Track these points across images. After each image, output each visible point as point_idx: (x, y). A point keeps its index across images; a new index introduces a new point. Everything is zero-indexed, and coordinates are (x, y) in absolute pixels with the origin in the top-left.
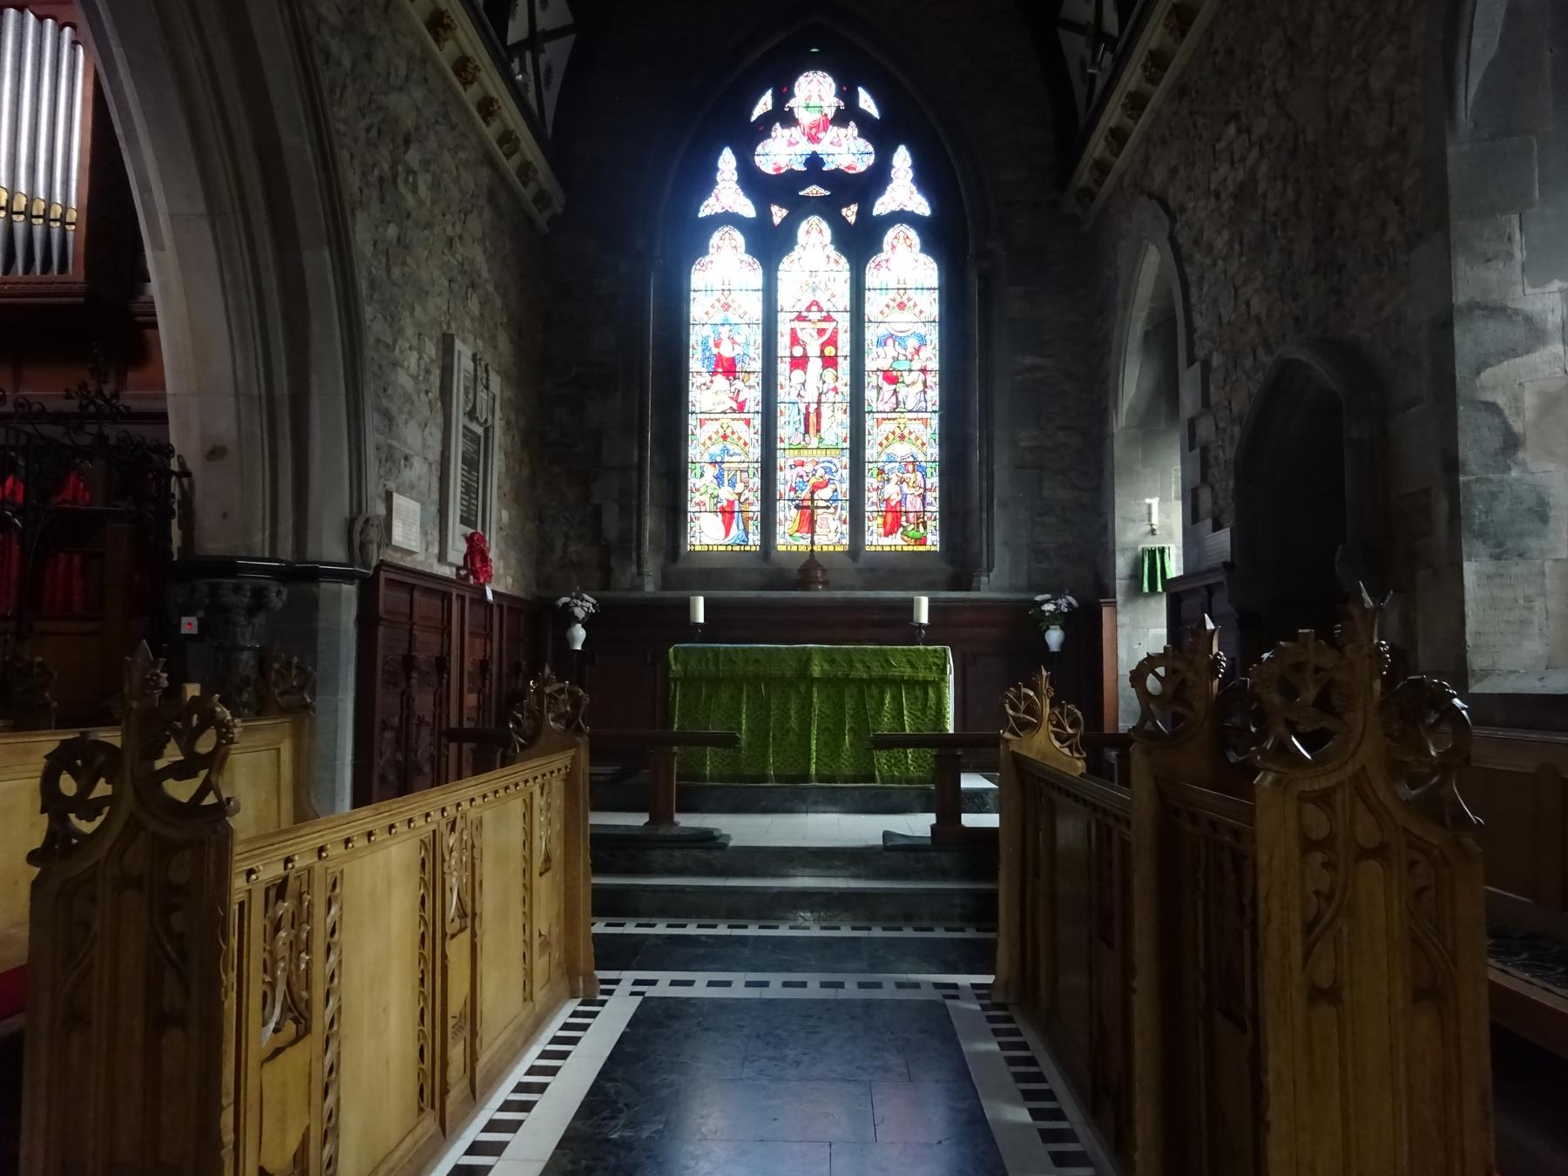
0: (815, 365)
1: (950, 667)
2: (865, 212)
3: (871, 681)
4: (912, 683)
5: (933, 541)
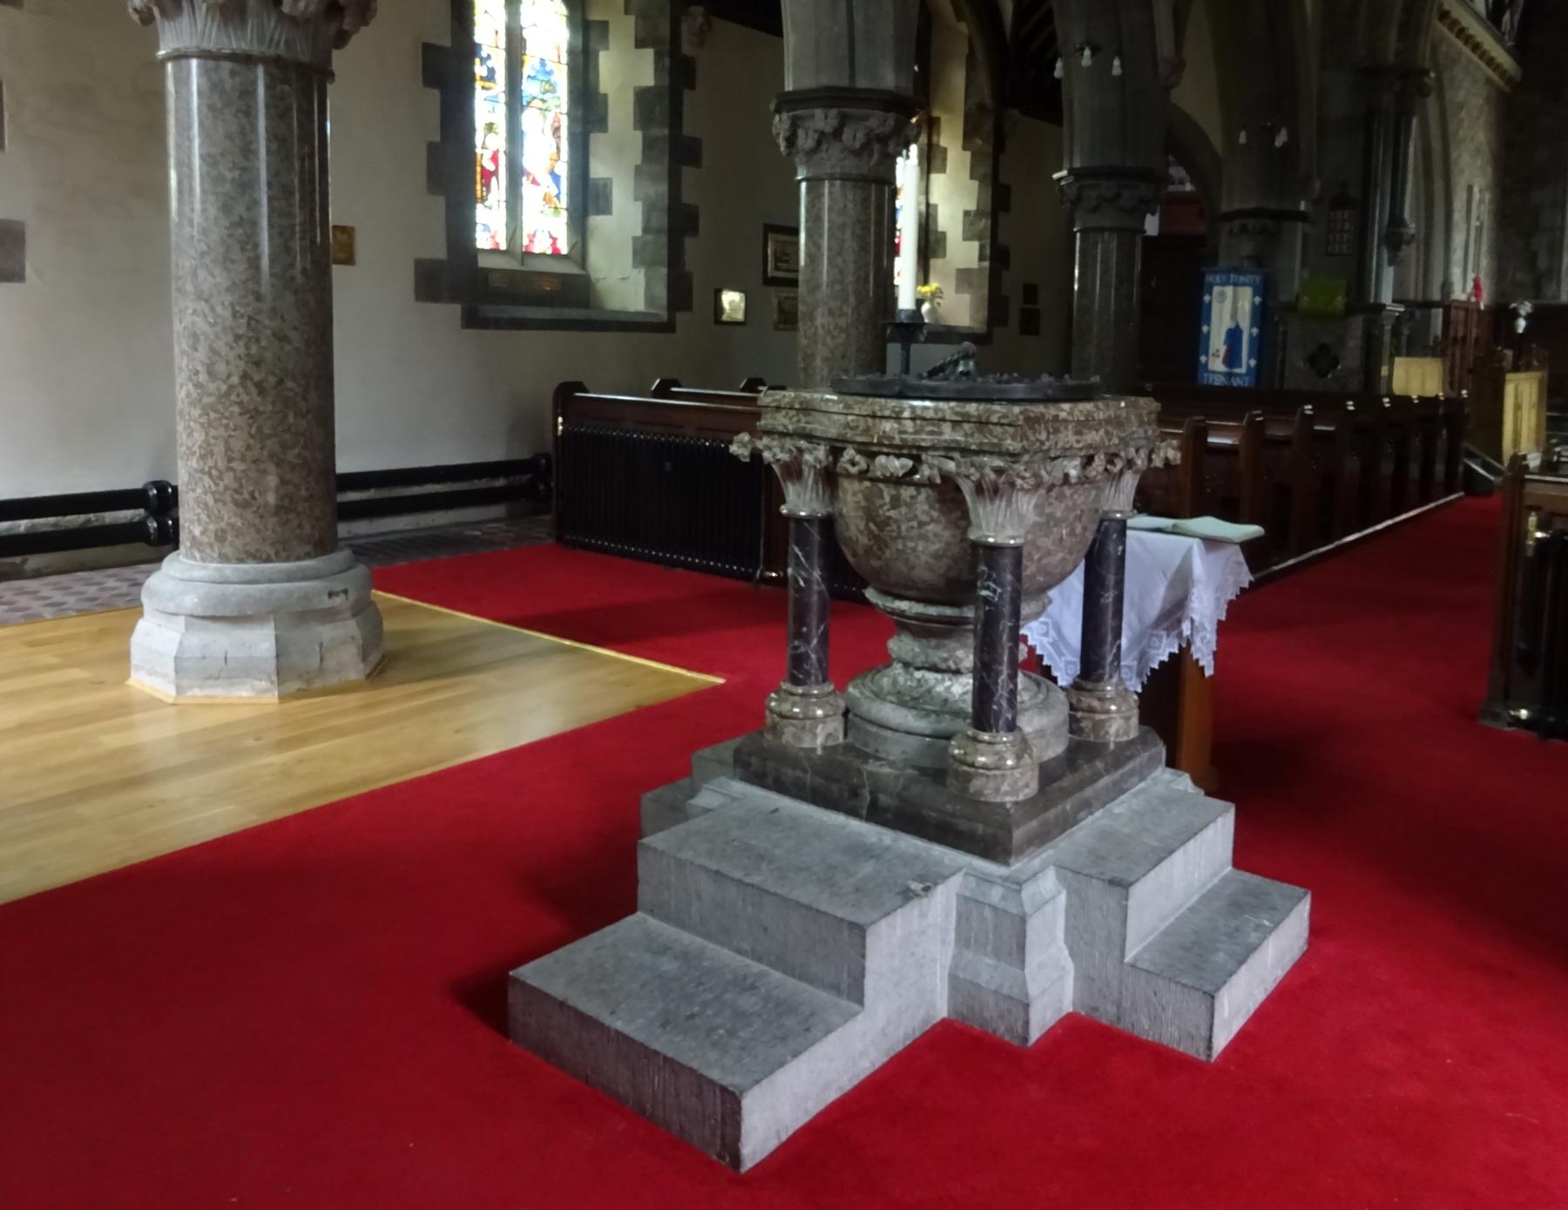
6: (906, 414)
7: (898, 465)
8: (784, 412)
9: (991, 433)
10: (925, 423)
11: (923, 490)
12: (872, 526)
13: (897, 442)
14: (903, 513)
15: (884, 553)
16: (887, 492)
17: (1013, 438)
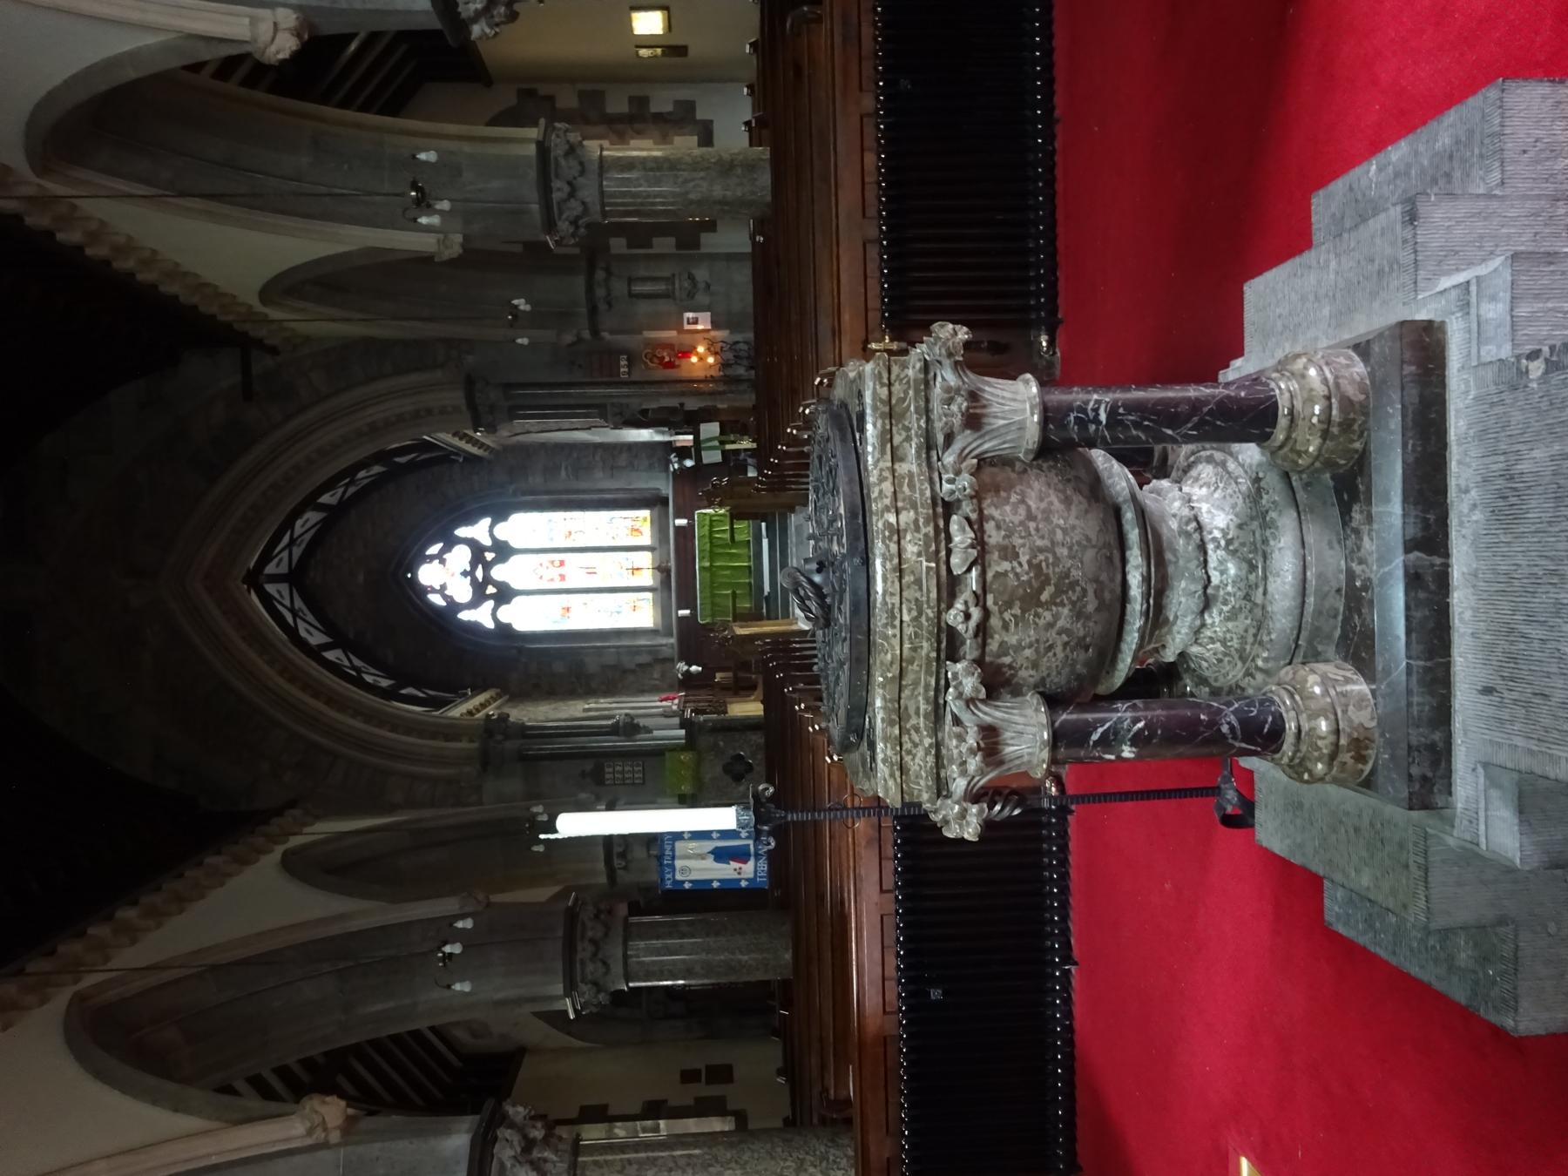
0: (562, 570)
1: (704, 511)
3: (711, 542)
4: (711, 526)
5: (646, 513)
6: (892, 518)
7: (961, 537)
8: (907, 758)
9: (904, 400)
10: (900, 496)
11: (986, 512)
12: (1045, 596)
13: (930, 529)
14: (1021, 541)
15: (1077, 583)
16: (999, 566)
17: (904, 366)
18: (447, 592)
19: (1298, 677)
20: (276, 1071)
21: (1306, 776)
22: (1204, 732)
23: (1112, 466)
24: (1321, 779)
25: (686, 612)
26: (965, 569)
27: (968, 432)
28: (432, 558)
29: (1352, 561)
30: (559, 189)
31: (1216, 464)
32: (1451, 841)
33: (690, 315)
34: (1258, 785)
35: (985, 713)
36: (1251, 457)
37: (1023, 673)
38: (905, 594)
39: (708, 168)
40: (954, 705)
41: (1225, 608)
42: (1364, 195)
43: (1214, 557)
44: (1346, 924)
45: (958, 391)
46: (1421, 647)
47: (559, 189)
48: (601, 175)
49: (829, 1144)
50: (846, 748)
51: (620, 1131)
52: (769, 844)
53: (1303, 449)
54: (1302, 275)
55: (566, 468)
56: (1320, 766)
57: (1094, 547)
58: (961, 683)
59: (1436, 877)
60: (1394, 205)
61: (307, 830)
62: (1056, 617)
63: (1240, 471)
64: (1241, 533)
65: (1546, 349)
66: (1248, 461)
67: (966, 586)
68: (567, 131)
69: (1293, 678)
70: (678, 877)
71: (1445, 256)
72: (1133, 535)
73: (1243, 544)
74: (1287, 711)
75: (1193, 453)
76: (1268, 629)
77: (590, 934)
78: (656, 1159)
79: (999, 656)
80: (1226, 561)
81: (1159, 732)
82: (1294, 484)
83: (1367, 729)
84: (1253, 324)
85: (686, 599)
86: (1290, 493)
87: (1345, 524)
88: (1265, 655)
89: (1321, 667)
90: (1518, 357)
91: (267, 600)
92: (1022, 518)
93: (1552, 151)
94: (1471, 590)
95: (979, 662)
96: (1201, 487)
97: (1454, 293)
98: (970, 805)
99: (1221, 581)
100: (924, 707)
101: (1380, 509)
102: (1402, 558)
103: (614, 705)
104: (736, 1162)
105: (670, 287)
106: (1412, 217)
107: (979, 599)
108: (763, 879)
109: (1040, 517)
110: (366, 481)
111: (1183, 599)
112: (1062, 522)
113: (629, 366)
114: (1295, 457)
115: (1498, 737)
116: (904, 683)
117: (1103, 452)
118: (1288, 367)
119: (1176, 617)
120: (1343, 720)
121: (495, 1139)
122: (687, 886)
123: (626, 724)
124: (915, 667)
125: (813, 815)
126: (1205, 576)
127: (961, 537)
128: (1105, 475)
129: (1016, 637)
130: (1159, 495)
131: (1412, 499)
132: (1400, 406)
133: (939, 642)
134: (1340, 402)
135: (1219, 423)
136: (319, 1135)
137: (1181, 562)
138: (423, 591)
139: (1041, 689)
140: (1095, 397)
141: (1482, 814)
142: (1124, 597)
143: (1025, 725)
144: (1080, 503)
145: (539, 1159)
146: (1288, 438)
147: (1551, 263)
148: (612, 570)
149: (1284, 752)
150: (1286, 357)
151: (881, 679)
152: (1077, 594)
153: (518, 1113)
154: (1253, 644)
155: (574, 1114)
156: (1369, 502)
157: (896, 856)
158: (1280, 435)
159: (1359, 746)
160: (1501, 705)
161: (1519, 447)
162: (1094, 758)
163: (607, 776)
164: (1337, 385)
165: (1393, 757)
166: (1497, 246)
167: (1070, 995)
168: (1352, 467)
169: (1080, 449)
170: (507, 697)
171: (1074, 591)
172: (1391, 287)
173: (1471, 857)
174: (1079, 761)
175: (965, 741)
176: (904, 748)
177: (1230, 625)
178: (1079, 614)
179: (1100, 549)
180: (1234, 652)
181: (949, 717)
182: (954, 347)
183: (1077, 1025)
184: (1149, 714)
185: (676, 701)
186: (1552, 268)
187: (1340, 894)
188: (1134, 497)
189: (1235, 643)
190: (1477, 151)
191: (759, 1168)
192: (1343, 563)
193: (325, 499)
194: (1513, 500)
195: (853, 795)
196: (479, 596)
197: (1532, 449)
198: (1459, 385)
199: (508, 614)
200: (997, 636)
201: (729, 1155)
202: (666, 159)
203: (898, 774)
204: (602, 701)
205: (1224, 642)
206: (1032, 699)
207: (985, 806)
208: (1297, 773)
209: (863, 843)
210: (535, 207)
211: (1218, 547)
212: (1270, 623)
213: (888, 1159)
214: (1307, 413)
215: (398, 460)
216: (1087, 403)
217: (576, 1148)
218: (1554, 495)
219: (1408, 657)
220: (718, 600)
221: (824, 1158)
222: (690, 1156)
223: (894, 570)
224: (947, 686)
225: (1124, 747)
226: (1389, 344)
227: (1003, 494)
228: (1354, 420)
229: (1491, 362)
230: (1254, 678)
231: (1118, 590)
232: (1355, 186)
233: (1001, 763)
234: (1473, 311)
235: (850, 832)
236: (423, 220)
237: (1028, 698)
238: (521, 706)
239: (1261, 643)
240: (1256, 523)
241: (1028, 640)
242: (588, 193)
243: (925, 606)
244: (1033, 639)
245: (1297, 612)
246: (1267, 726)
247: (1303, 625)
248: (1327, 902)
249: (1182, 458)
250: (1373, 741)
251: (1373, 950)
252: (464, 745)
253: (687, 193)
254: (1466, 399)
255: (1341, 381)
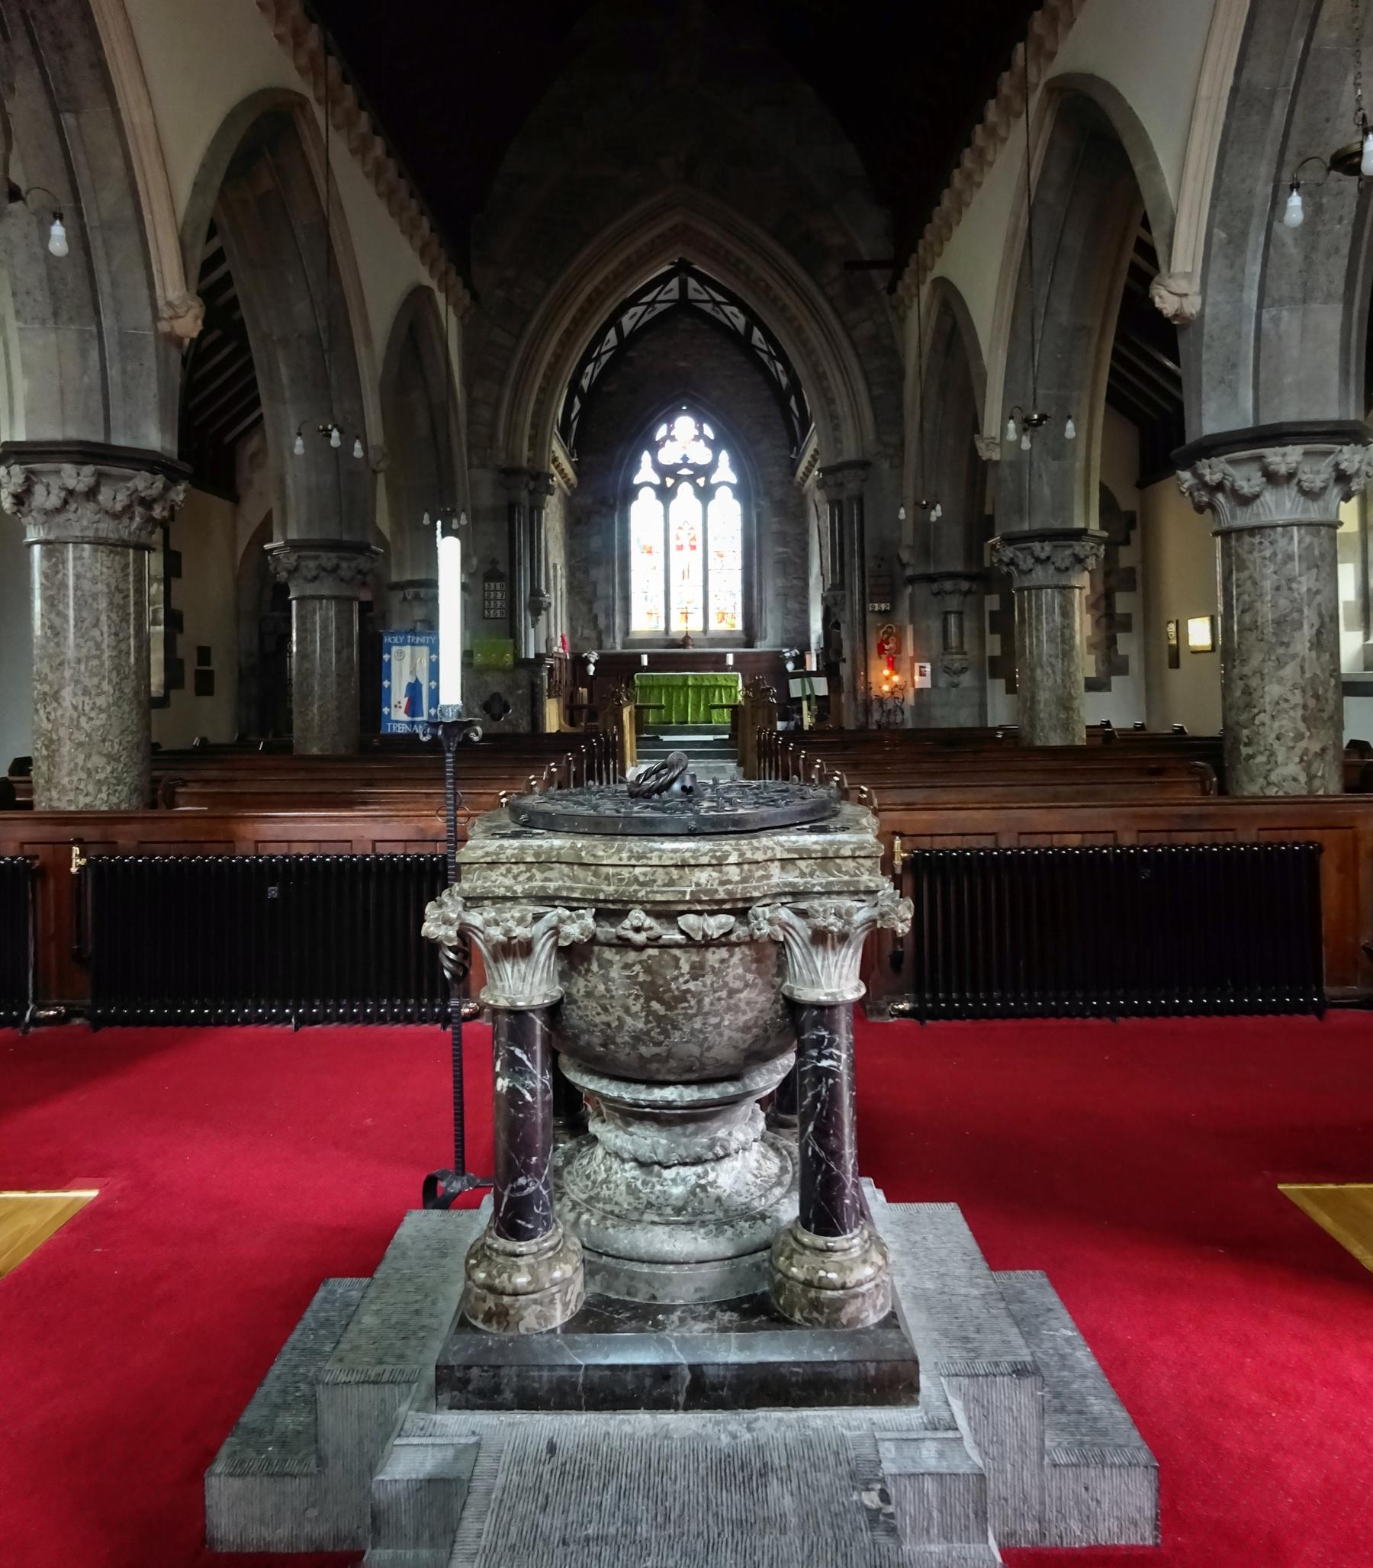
0: (687, 548)
2: (707, 481)
5: (739, 626)
6: (733, 858)
7: (715, 925)
8: (503, 869)
10: (754, 867)
11: (737, 949)
12: (655, 1005)
13: (722, 895)
14: (709, 983)
15: (668, 1036)
17: (871, 871)
18: (668, 442)
19: (570, 1255)
20: (228, 274)
21: (473, 1261)
22: (519, 1160)
23: (779, 1073)
24: (469, 1277)
25: (645, 661)
26: (683, 928)
27: (810, 932)
28: (701, 429)
29: (683, 1312)
30: (1043, 548)
31: (779, 1177)
32: (403, 1409)
33: (928, 668)
34: (465, 1214)
35: (544, 945)
36: (786, 1211)
37: (581, 983)
38: (660, 870)
39: (1065, 687)
40: (553, 915)
41: (639, 1183)
42: (1043, 1323)
43: (690, 1173)
44: (325, 1300)
45: (848, 923)
46: (596, 1380)
47: (1043, 549)
48: (1056, 587)
49: (133, 786)
50: (515, 810)
51: (156, 589)
52: (424, 735)
53: (794, 1261)
54: (964, 1261)
55: (783, 553)
56: (482, 1275)
57: (702, 1054)
58: (574, 922)
59: (370, 1392)
60: (1032, 1354)
61: (450, 309)
62: (635, 1016)
63: (772, 1200)
64: (712, 1200)
65: (890, 1509)
66: (782, 1208)
67: (667, 929)
68: (1097, 556)
69: (569, 1250)
70: (394, 649)
71: (983, 1406)
72: (712, 1093)
73: (701, 1202)
74: (537, 1243)
75: (790, 1154)
76: (618, 1225)
77: (344, 565)
78: (128, 622)
79: (598, 960)
80: (685, 1184)
81: (521, 1115)
82: (760, 1254)
83: (518, 1324)
84: (918, 1212)
85: (659, 662)
86: (751, 1250)
87: (719, 1304)
88: (593, 1222)
89: (580, 1278)
90: (883, 1481)
91: (664, 279)
92: (731, 985)
93: (1088, 1517)
94: (651, 1432)
95: (594, 940)
96: (758, 1161)
97: (946, 1415)
98: (456, 928)
99: (665, 1180)
100: (552, 886)
101: (733, 1341)
102: (685, 1362)
103: (559, 593)
104: (120, 698)
105: (954, 651)
106: (1020, 1371)
107: (654, 942)
108: (390, 729)
109: (732, 1001)
110: (773, 370)
111: (648, 1141)
112: (726, 1023)
113: (880, 612)
114: (786, 1254)
115: (506, 1458)
116: (576, 867)
117: (792, 1064)
118: (874, 1247)
119: (631, 1134)
120: (527, 1300)
121: (154, 473)
122: (386, 657)
123: (541, 603)
124: (590, 878)
125: (451, 777)
126: (671, 1163)
127: (715, 925)
128: (770, 1066)
129: (616, 977)
130: (751, 1119)
131: (742, 1372)
132: (835, 1359)
133: (613, 902)
134: (839, 1299)
135: (819, 1177)
136: (166, 312)
137: (684, 1140)
138: (670, 420)
139: (565, 1000)
140: (844, 1056)
141: (430, 1440)
142: (653, 1083)
143: (532, 984)
144: (744, 1041)
145: (133, 513)
146: (805, 1246)
147: (976, 1515)
148: (686, 594)
149: (497, 1240)
150: (884, 1245)
151: (579, 845)
152: (656, 1036)
153: (178, 494)
154: (604, 1210)
155: (174, 546)
156: (741, 1329)
157: (409, 856)
158: (808, 1238)
159: (501, 1316)
160: (537, 1462)
161: (794, 1484)
162: (498, 1051)
163: (492, 584)
164: (856, 1296)
165: (489, 1350)
166: (993, 1459)
167: (265, 1022)
168: (778, 1312)
169: (796, 1042)
170: (569, 494)
171: (659, 1034)
172: (953, 1350)
173: (387, 1429)
174: (495, 1035)
175: (518, 925)
176: (513, 866)
177: (623, 1188)
178: (637, 1038)
179: (699, 1060)
180: (596, 1191)
181: (541, 910)
182: (890, 919)
183: (236, 1029)
184: (538, 1106)
185: (561, 651)
186: (972, 1516)
187: (355, 1294)
188: (749, 1094)
189: (605, 1193)
190: (1087, 1439)
191: (113, 718)
192: (681, 1302)
193: (757, 334)
194: (740, 1477)
195: (469, 816)
196: (663, 471)
197: (792, 1495)
198: (856, 1419)
199: (647, 496)
200: (618, 958)
201: (127, 691)
202: (1072, 648)
203: (489, 859)
204: (564, 581)
205: (606, 1181)
206: (556, 991)
207: (455, 943)
208: (476, 1252)
209: (421, 825)
210: (1026, 527)
211: (699, 1177)
212: (623, 1228)
213: (115, 843)
214: (829, 1266)
215: (793, 399)
216: (838, 1048)
217: (141, 548)
218: (744, 1518)
219: (587, 1367)
220: (656, 692)
221: (119, 781)
222: (128, 653)
223: (683, 860)
224: (571, 909)
225: (507, 1080)
226: (896, 1349)
227: (754, 966)
228: (821, 1313)
229: (878, 1451)
230: (570, 1211)
231: (660, 1077)
232: (1051, 1314)
233: (496, 960)
234: (929, 1434)
235: (434, 813)
236: (1011, 425)
237: (558, 987)
238: (559, 506)
239: (604, 1218)
240: (720, 1214)
241: (613, 988)
242: (1040, 575)
243: (648, 889)
244: (614, 993)
245: (634, 1255)
246: (523, 1223)
247: (621, 1261)
248: (347, 1281)
249: (785, 1142)
250: (505, 1330)
251: (299, 1326)
252: (526, 453)
253: (1042, 667)
254: (842, 1426)
255: (860, 1299)
